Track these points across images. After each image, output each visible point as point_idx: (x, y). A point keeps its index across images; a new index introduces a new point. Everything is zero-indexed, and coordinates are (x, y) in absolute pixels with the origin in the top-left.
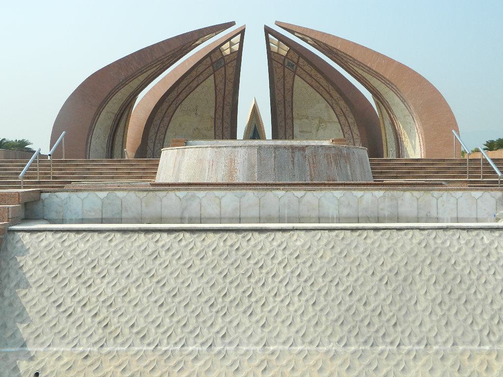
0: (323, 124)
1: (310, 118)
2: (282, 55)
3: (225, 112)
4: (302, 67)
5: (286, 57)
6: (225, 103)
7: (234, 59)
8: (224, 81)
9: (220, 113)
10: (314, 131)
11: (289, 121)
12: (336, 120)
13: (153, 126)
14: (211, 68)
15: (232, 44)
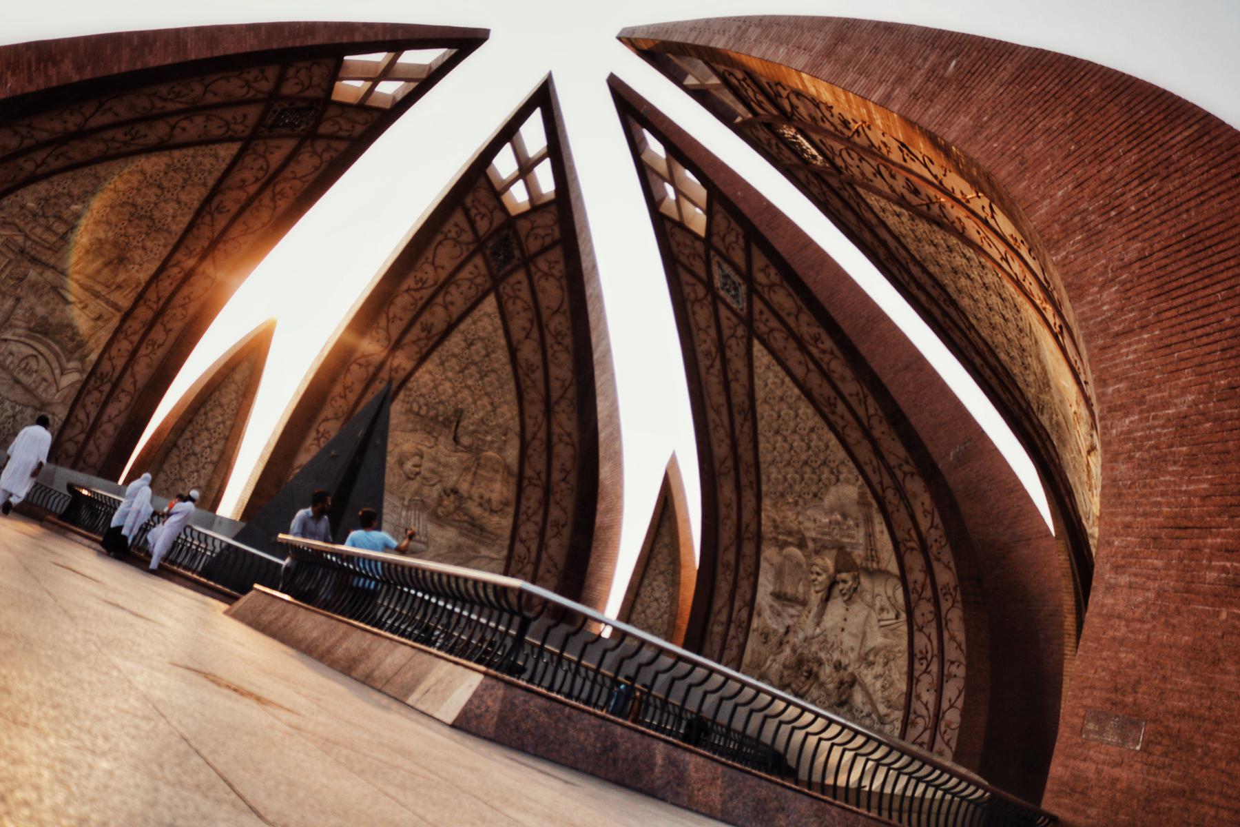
0: (844, 575)
1: (811, 545)
2: (696, 236)
3: (556, 464)
4: (766, 296)
5: (708, 240)
6: (556, 429)
7: (554, 244)
8: (535, 334)
9: (537, 462)
10: (815, 599)
11: (748, 548)
12: (893, 567)
13: (313, 434)
14: (478, 260)
15: (526, 169)
